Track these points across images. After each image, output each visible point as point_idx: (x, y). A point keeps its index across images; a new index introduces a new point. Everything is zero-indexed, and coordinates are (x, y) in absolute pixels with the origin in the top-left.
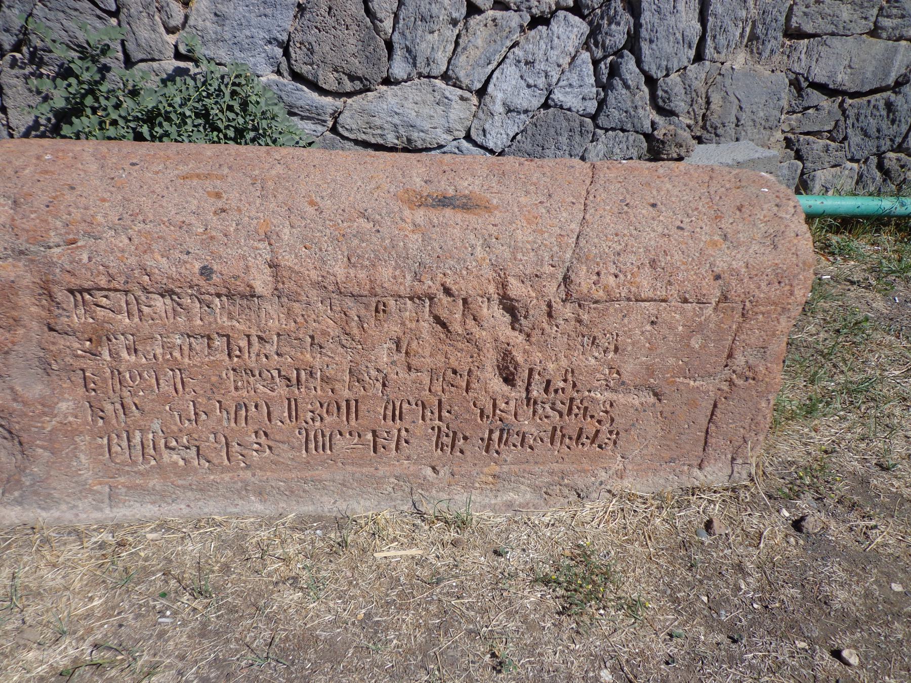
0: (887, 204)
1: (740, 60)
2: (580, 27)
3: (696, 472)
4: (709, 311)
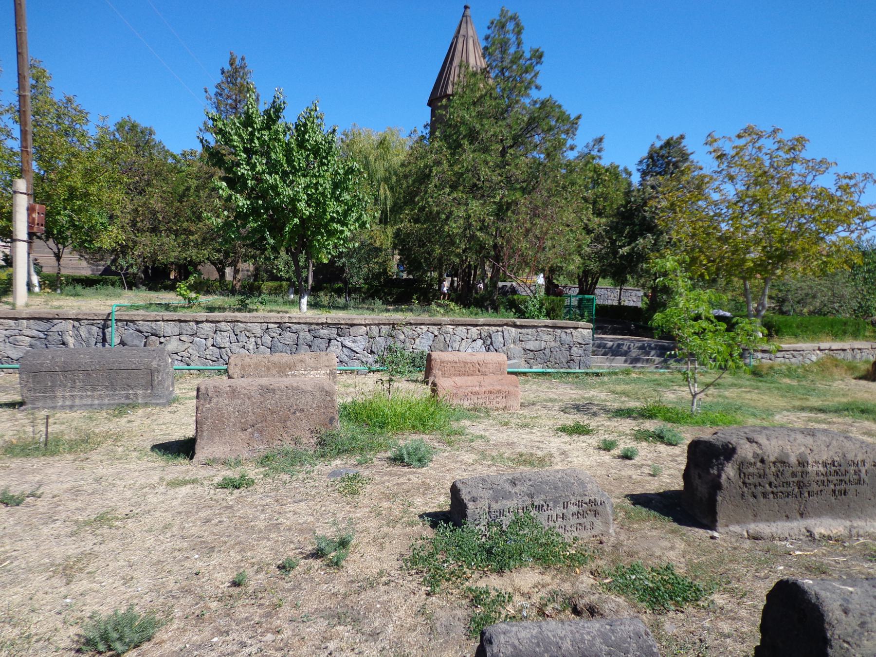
0: (544, 370)
1: (512, 346)
2: (481, 341)
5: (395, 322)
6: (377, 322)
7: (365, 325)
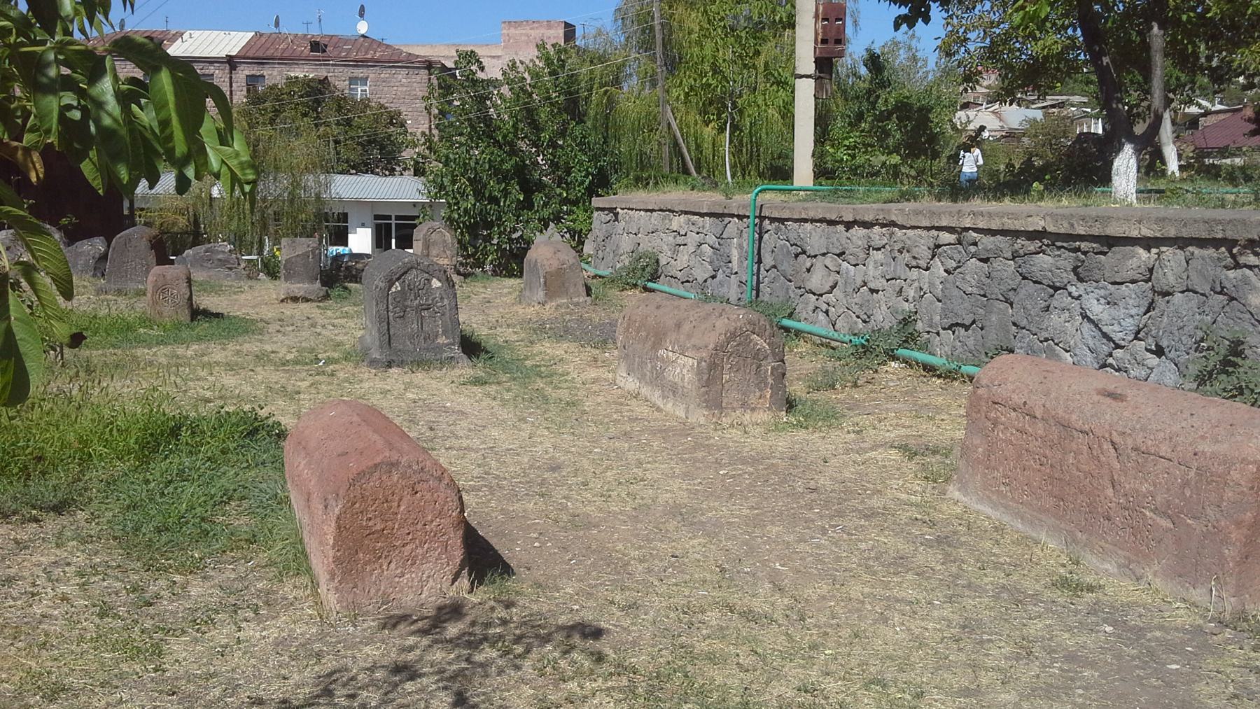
3: (1191, 589)
4: (1192, 474)
5: (1230, 234)
6: (1172, 233)
7: (1148, 243)
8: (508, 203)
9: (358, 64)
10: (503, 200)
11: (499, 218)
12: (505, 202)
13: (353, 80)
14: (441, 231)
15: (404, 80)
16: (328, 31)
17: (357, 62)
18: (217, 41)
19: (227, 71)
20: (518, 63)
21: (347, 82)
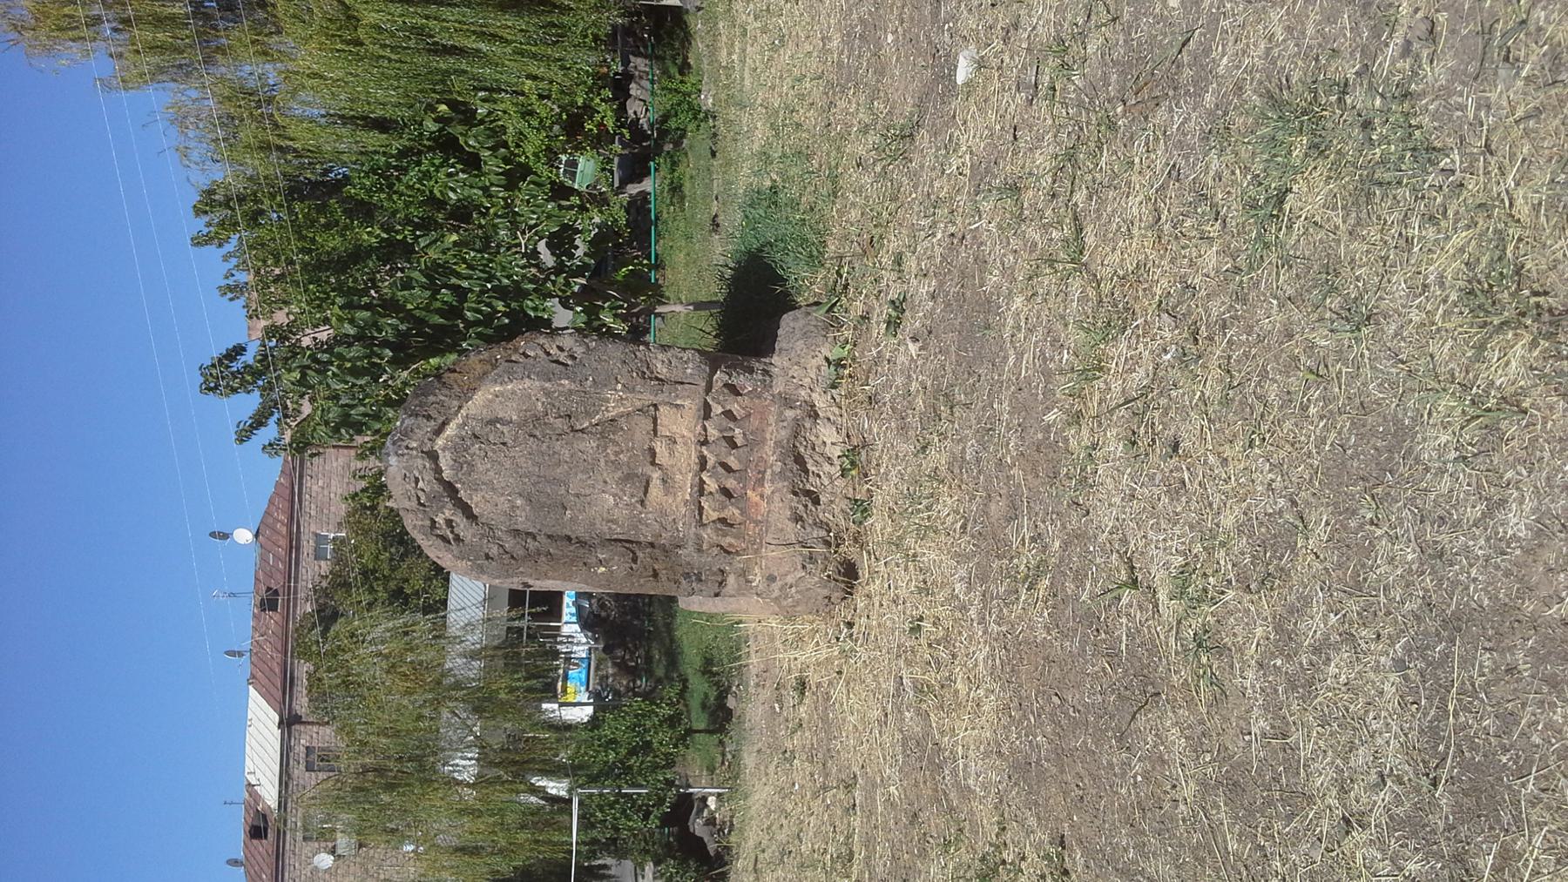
8: (462, 269)
9: (294, 545)
10: (454, 281)
11: (501, 292)
12: (459, 276)
13: (319, 555)
14: (459, 448)
15: (321, 483)
16: (249, 585)
17: (291, 547)
18: (260, 738)
19: (302, 728)
20: (231, 282)
21: (323, 563)
